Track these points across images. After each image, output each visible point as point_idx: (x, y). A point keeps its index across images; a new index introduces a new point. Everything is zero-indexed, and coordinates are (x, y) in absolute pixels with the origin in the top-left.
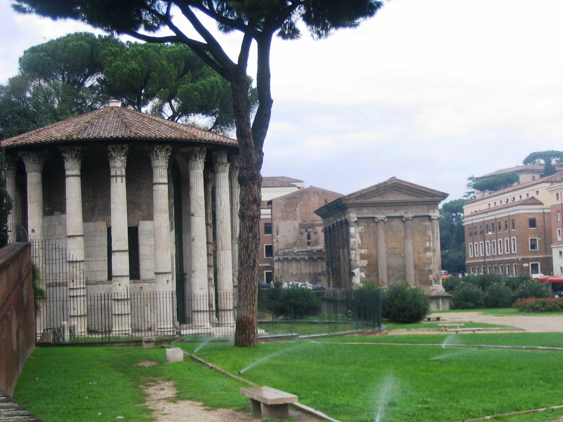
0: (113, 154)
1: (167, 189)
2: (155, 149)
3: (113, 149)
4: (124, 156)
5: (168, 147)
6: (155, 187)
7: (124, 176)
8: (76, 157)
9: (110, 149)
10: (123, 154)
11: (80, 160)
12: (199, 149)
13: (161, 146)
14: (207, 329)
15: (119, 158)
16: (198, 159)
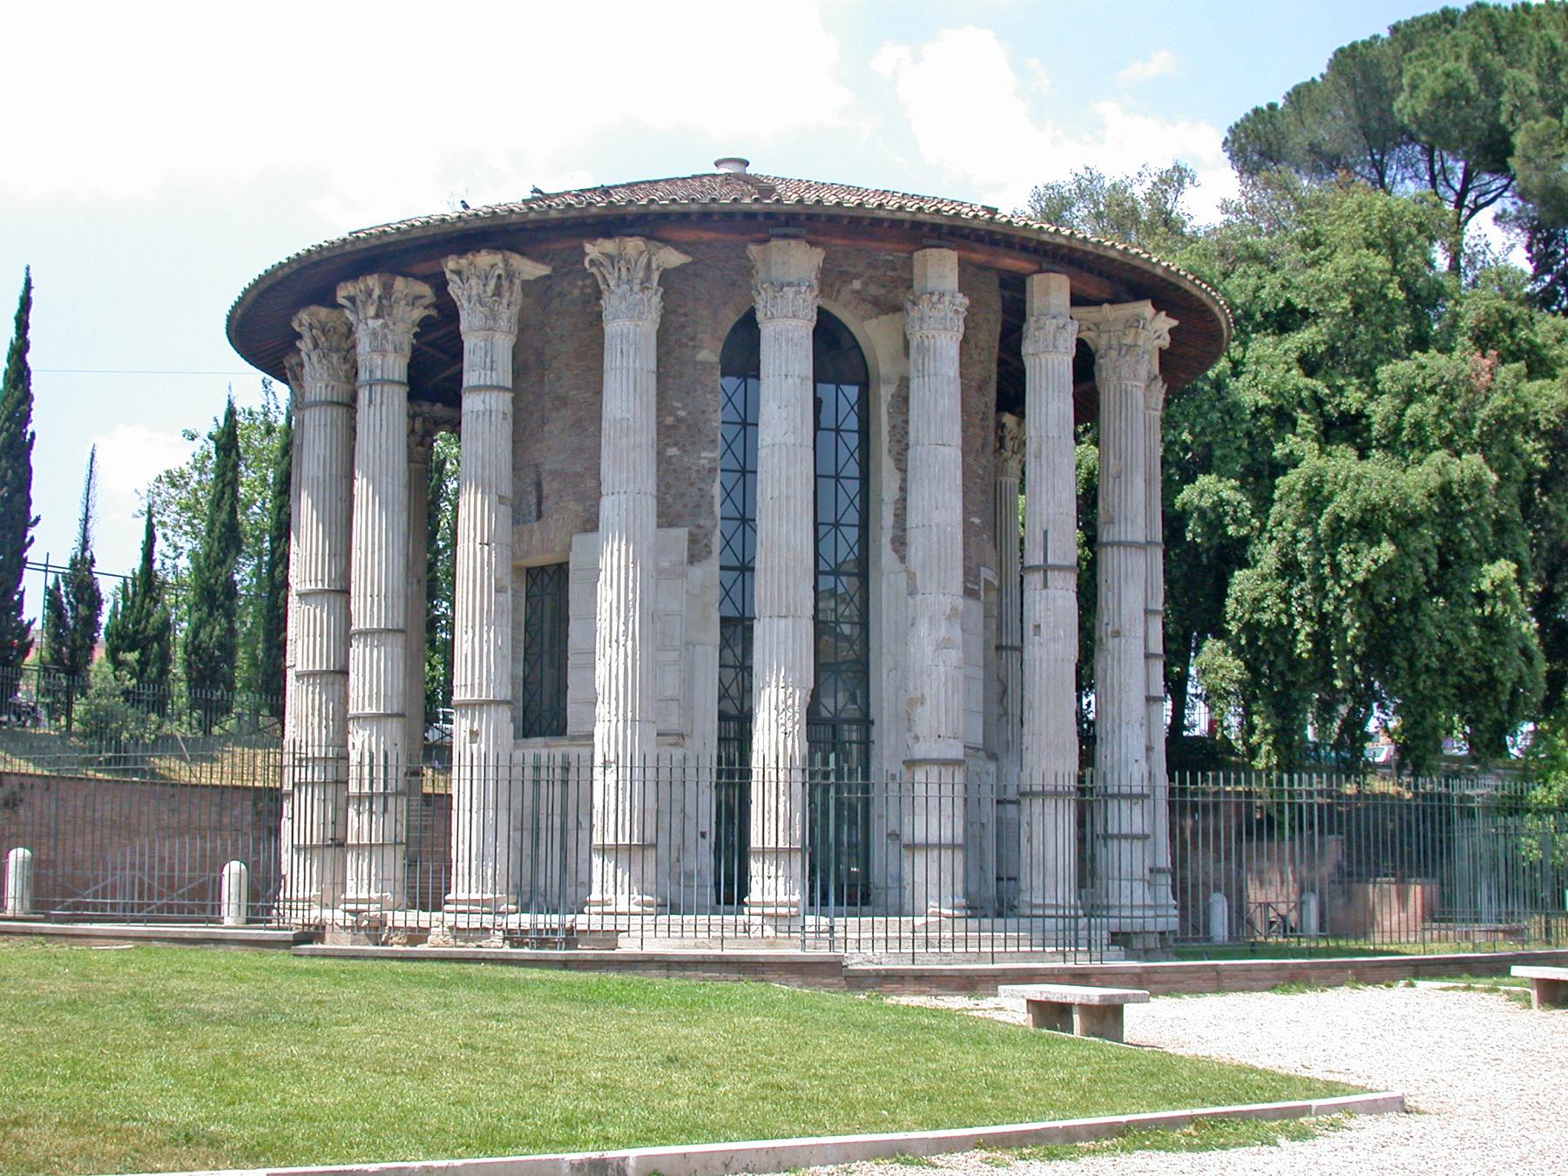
0: (351, 317)
1: (509, 408)
2: (448, 275)
3: (352, 299)
4: (377, 316)
5: (485, 259)
6: (471, 404)
7: (393, 382)
8: (316, 346)
9: (341, 301)
10: (372, 311)
11: (335, 358)
12: (609, 246)
13: (463, 262)
14: (616, 914)
15: (362, 326)
16: (612, 283)
